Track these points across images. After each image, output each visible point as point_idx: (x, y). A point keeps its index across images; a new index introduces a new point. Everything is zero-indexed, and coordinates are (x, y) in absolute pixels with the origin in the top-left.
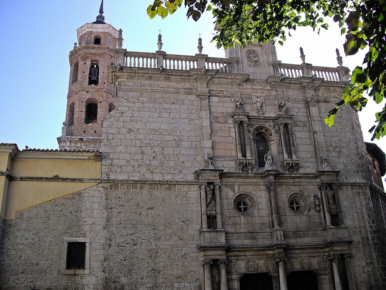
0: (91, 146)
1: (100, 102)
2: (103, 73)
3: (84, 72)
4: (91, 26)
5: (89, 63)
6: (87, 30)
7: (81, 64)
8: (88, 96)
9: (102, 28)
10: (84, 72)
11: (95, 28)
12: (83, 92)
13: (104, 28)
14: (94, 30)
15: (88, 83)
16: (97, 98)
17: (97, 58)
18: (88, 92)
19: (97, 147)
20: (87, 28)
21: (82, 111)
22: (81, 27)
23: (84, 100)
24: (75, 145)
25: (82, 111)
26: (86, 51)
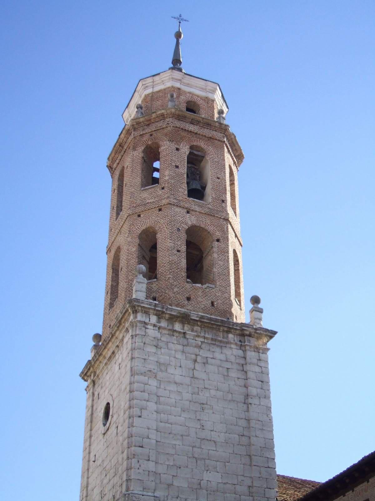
0: (207, 336)
1: (218, 240)
2: (218, 178)
3: (177, 167)
4: (179, 78)
5: (185, 150)
6: (169, 84)
7: (166, 147)
8: (191, 220)
9: (202, 89)
10: (177, 167)
11: (188, 85)
12: (178, 210)
13: (206, 89)
14: (184, 88)
15: (186, 192)
16: (210, 228)
17: (202, 144)
18: (188, 212)
19: (221, 341)
20: (169, 79)
21: (178, 251)
22: (153, 76)
23: (183, 227)
24: (170, 327)
25: (178, 251)
26: (178, 124)
